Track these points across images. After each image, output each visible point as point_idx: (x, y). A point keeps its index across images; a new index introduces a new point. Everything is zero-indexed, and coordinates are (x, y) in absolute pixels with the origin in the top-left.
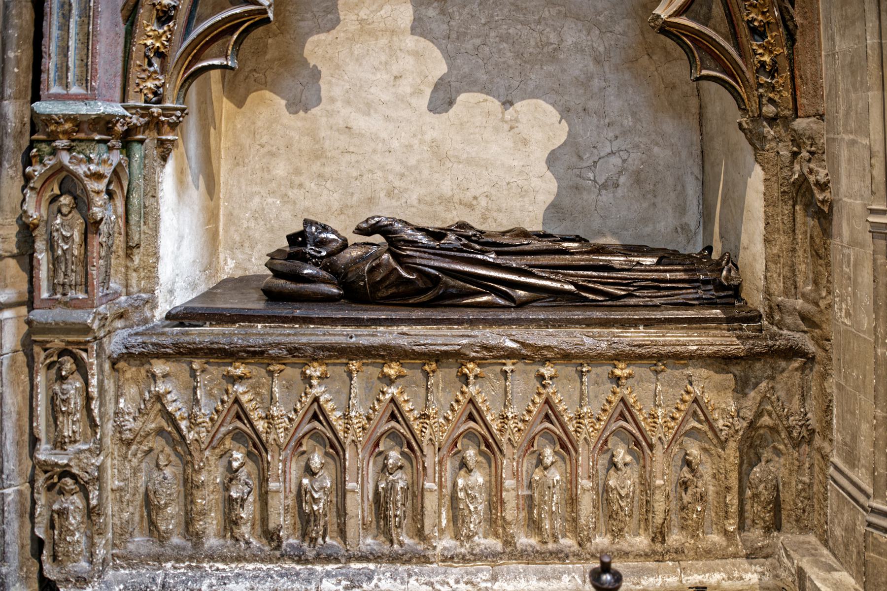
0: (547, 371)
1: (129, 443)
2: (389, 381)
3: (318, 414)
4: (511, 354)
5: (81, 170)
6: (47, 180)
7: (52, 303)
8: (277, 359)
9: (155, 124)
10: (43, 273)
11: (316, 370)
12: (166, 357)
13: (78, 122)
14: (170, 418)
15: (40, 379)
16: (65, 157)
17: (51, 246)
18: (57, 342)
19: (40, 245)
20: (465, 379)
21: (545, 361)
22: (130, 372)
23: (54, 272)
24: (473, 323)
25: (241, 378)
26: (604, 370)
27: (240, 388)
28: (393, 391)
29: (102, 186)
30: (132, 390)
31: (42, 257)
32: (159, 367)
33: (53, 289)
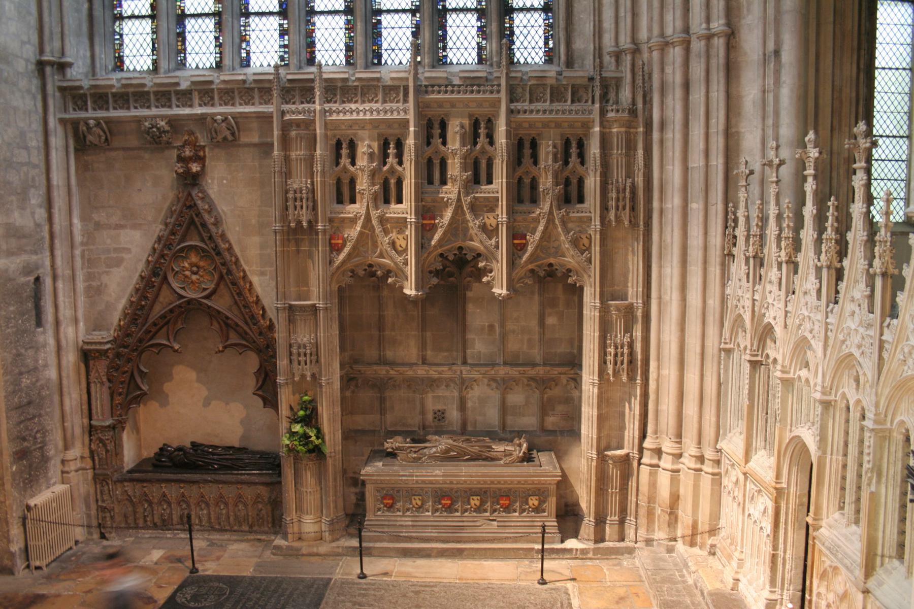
0: (220, 486)
1: (119, 502)
3: (164, 495)
4: (210, 482)
5: (103, 438)
6: (96, 440)
7: (99, 469)
9: (120, 422)
10: (97, 462)
11: (163, 485)
13: (102, 427)
14: (129, 496)
15: (98, 486)
16: (100, 435)
17: (98, 455)
18: (101, 478)
19: (96, 455)
20: (200, 487)
21: (220, 483)
22: (119, 485)
23: (99, 461)
24: (202, 474)
25: (145, 487)
26: (235, 486)
27: (145, 489)
28: (182, 490)
29: (109, 441)
30: (120, 489)
31: (96, 458)
33: (99, 465)
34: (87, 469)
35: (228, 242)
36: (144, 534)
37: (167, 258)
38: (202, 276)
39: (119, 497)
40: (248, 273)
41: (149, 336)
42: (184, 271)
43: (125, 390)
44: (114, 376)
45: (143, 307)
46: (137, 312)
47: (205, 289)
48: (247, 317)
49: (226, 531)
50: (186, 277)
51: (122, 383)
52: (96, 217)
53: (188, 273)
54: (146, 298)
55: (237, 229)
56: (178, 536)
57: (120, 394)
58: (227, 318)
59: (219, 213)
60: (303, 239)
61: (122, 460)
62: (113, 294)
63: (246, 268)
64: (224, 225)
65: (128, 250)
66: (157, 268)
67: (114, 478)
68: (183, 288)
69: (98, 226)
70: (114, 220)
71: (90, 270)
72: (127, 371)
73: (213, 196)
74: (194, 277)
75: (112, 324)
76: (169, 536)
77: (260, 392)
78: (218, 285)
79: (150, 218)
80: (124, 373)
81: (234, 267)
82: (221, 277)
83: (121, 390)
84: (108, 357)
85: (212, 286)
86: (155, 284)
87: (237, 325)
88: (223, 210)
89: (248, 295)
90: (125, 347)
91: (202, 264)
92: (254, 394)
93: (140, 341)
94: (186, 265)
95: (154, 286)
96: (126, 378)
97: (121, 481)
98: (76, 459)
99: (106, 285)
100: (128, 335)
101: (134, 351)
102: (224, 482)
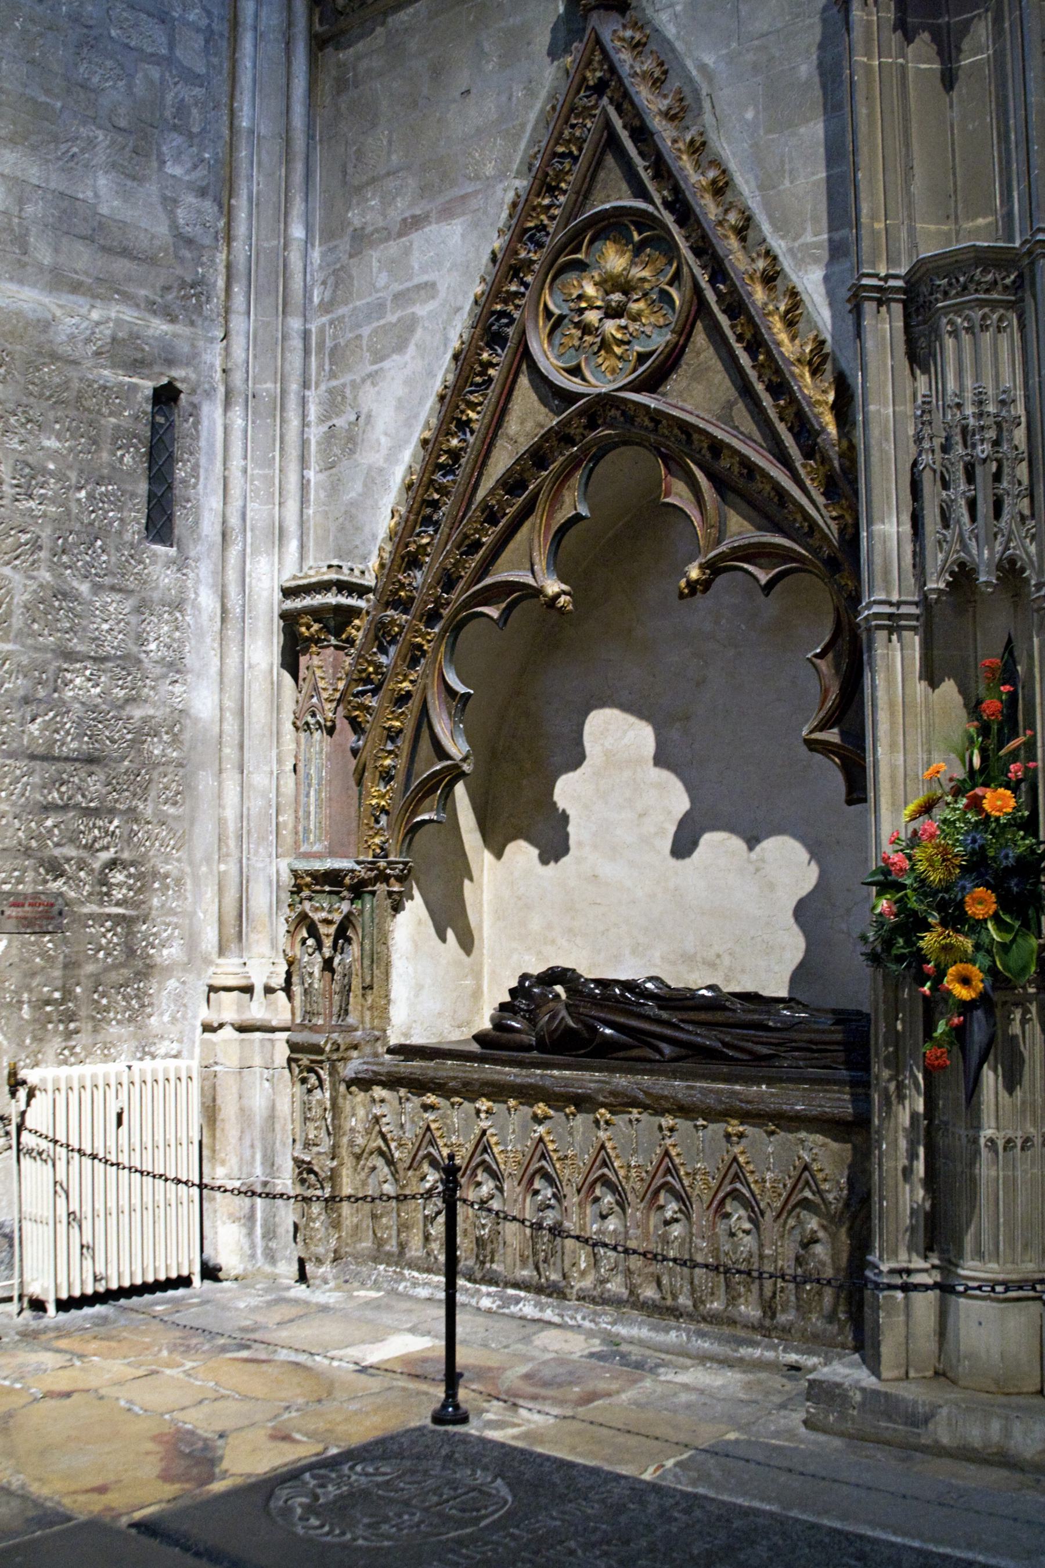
0: (667, 1121)
2: (538, 1120)
8: (456, 1093)
12: (384, 1085)
32: (378, 1092)
34: (273, 1030)
35: (715, 163)
36: (415, 1285)
37: (529, 279)
38: (635, 318)
39: (360, 1141)
40: (786, 264)
41: (473, 562)
42: (581, 311)
43: (401, 763)
44: (367, 709)
45: (455, 455)
46: (437, 476)
47: (642, 358)
48: (781, 428)
49: (675, 1313)
50: (586, 329)
51: (393, 735)
52: (355, 218)
53: (592, 317)
54: (464, 425)
55: (749, 115)
56: (514, 1309)
57: (387, 776)
58: (717, 447)
59: (691, 80)
60: (965, 28)
61: (382, 1011)
62: (383, 439)
63: (778, 245)
64: (708, 118)
65: (429, 288)
66: (502, 314)
67: (350, 1069)
68: (575, 371)
69: (361, 240)
70: (401, 208)
71: (334, 383)
72: (409, 695)
73: (671, 31)
74: (611, 327)
75: (374, 537)
76: (486, 1303)
77: (833, 736)
78: (685, 332)
79: (489, 170)
80: (404, 698)
81: (734, 243)
82: (699, 307)
83: (388, 762)
84: (351, 641)
85: (660, 341)
86: (491, 372)
87: (750, 469)
88: (703, 68)
89: (783, 337)
90: (404, 605)
91: (638, 272)
92: (812, 745)
93: (448, 581)
94: (590, 290)
95: (490, 379)
96: (403, 721)
97: (364, 1083)
98: (248, 990)
99: (369, 416)
100: (413, 562)
101: (432, 618)
102: (684, 1110)
